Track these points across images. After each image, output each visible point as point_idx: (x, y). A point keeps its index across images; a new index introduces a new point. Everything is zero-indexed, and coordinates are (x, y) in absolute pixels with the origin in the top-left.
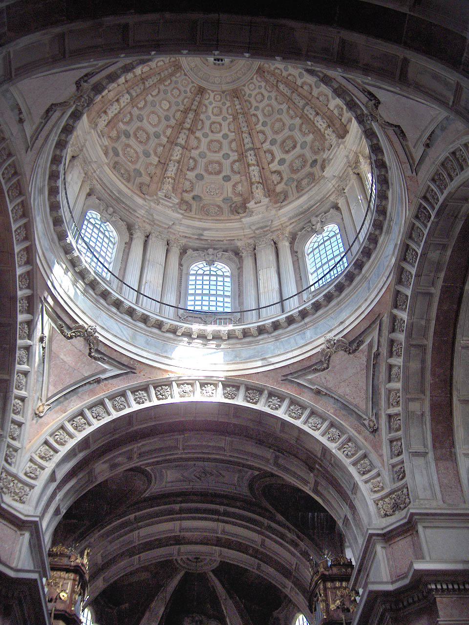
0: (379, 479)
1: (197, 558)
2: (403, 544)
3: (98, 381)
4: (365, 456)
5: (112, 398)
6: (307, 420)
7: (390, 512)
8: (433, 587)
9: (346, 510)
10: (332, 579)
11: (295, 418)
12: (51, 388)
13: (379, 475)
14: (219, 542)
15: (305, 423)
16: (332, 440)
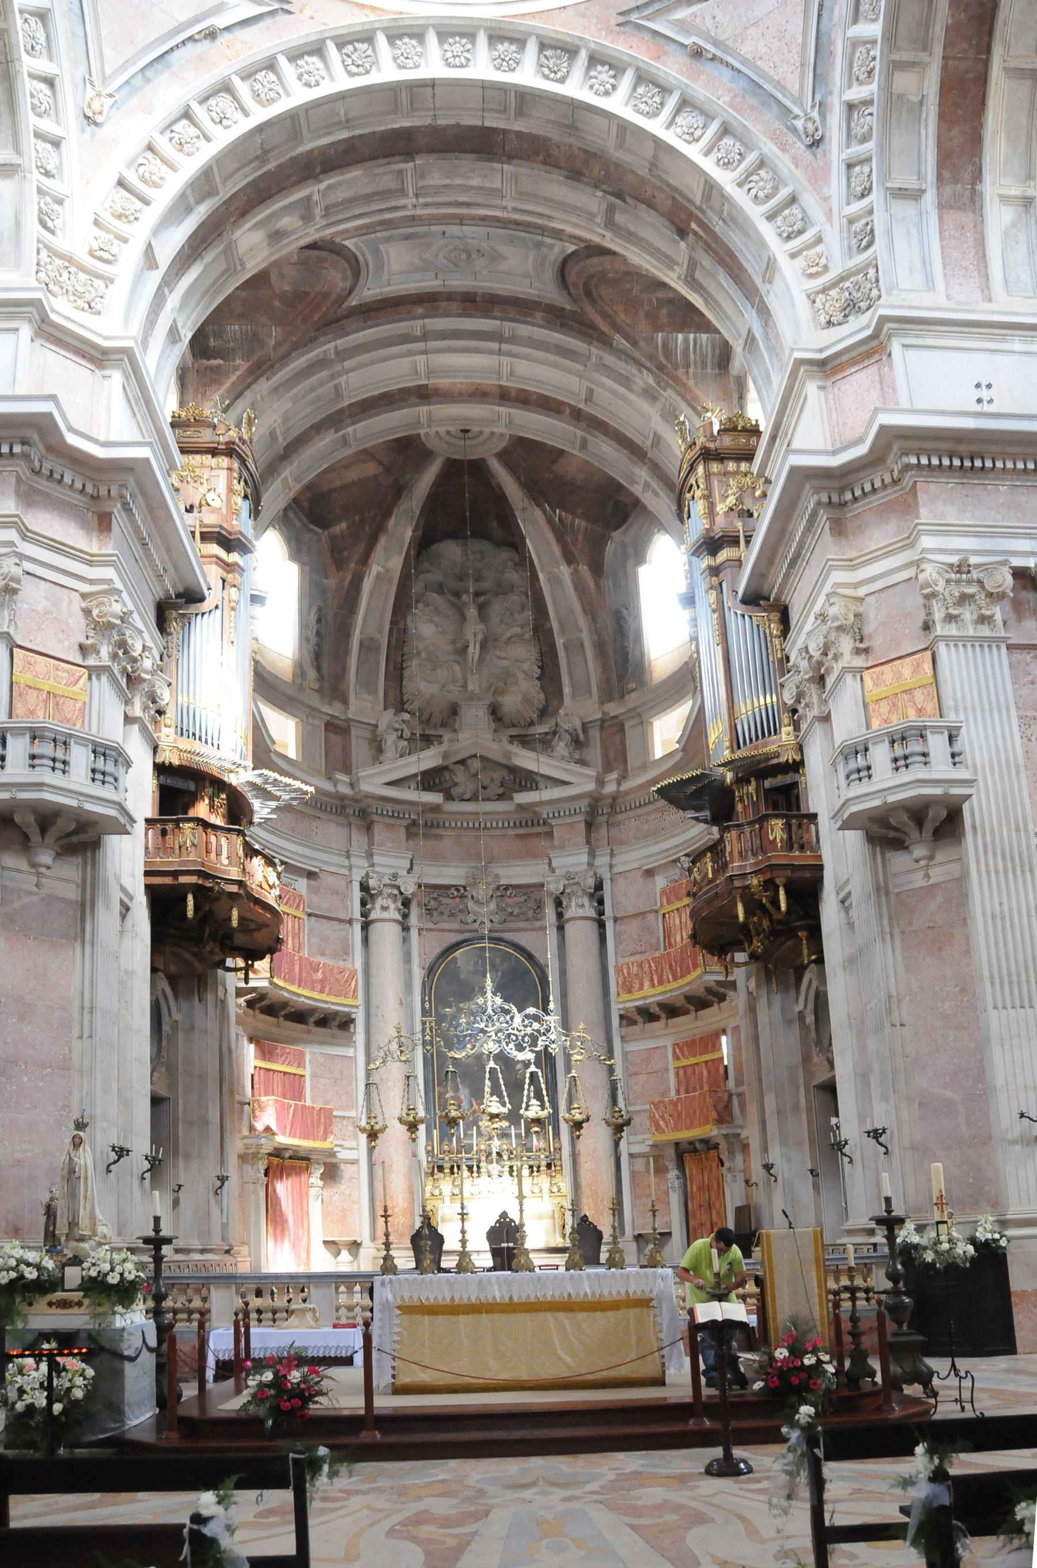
0: (819, 249)
1: (467, 431)
6: (674, 118)
7: (838, 317)
8: (914, 460)
9: (751, 318)
10: (719, 456)
11: (649, 115)
13: (819, 240)
14: (504, 396)
15: (670, 124)
16: (726, 164)
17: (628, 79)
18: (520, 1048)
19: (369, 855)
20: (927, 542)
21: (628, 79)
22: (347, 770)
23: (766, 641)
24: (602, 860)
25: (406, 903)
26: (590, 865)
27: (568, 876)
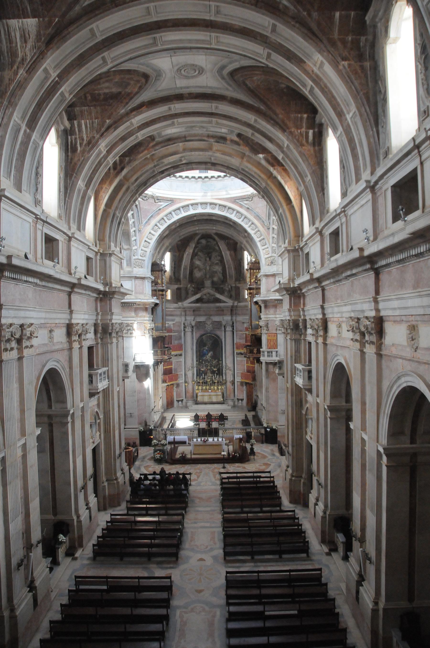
2: (271, 279)
3: (160, 209)
4: (264, 239)
5: (166, 216)
10: (253, 269)
12: (143, 219)
15: (243, 221)
17: (235, 212)
18: (214, 368)
20: (277, 316)
21: (235, 212)
23: (258, 311)
24: (234, 318)
26: (232, 319)
27: (227, 321)
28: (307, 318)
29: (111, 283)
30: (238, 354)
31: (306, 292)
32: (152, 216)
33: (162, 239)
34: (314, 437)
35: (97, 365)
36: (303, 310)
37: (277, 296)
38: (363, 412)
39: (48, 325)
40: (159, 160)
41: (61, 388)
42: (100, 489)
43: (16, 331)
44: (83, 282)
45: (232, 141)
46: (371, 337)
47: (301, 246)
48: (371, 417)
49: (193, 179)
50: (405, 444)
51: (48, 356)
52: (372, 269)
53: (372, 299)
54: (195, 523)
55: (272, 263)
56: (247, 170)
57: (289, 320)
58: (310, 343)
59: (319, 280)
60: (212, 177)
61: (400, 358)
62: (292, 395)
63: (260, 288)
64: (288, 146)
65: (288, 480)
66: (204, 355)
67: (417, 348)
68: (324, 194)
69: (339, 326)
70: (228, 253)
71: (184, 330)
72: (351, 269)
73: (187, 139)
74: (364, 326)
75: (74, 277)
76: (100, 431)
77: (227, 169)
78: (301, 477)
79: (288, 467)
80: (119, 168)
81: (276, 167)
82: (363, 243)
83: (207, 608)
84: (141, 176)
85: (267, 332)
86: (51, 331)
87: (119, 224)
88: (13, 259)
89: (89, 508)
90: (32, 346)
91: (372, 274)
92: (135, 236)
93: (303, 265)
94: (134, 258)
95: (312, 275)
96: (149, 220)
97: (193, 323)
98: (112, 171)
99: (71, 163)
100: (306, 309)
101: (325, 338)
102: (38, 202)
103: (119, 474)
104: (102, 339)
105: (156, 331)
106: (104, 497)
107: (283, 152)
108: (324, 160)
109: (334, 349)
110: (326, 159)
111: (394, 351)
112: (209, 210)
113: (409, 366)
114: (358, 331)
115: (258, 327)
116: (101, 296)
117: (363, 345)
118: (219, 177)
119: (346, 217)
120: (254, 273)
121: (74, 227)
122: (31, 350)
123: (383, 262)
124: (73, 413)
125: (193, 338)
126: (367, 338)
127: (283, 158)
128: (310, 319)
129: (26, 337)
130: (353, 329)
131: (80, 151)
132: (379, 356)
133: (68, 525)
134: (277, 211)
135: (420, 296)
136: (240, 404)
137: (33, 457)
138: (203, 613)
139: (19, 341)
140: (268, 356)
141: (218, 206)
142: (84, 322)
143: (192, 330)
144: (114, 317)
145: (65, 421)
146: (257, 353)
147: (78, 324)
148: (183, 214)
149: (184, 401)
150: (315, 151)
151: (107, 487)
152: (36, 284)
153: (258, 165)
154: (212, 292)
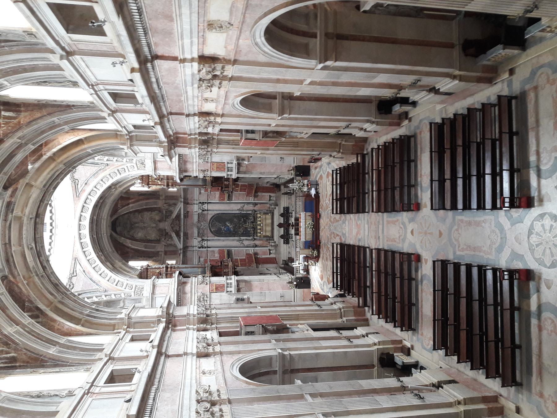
2: (159, 165)
3: (84, 271)
10: (149, 182)
17: (89, 197)
19: (194, 247)
20: (195, 161)
22: (177, 251)
24: (195, 202)
25: (203, 240)
28: (198, 131)
29: (158, 316)
30: (229, 199)
31: (172, 131)
32: (91, 279)
33: (114, 269)
34: (306, 130)
35: (237, 327)
36: (191, 135)
37: (176, 159)
38: (286, 82)
39: (198, 376)
40: (31, 271)
41: (257, 362)
42: (349, 325)
43: (203, 407)
44: (156, 343)
45: (12, 196)
46: (218, 69)
47: (127, 133)
48: (290, 75)
49: (53, 237)
50: (316, 44)
51: (228, 375)
52: (152, 62)
53: (182, 65)
54: (379, 238)
55: (142, 163)
56: (44, 183)
57: (199, 148)
58: (221, 130)
59: (161, 116)
60: (51, 218)
61: (238, 41)
62: (268, 150)
63: (168, 176)
64: (19, 138)
65: (343, 156)
66: (229, 229)
67: (229, 23)
68: (73, 106)
69: (206, 100)
70: (131, 205)
71: (205, 248)
72: (151, 83)
73: (7, 242)
74: (207, 74)
75: (151, 352)
76: (298, 324)
77: (43, 202)
78: (340, 144)
79: (331, 156)
80: (37, 313)
81: (43, 153)
82: (126, 69)
83: (456, 227)
84: (47, 289)
85: (209, 172)
86: (204, 373)
87: (97, 310)
88: (131, 414)
89: (367, 335)
90: (218, 391)
91: (157, 62)
92: (110, 295)
93: (146, 132)
94: (133, 295)
95: (156, 123)
96: (94, 282)
97: (200, 239)
98: (40, 320)
99: (28, 362)
100: (188, 132)
101: (216, 115)
102: (70, 394)
103: (335, 307)
104: (212, 324)
105: (205, 273)
106: (357, 320)
107: (26, 144)
108: (36, 102)
109: (227, 107)
110: (35, 100)
111: (231, 47)
112: (86, 223)
113: (246, 33)
114: (211, 81)
115: (204, 180)
116: (170, 326)
117: (225, 78)
118: (51, 212)
119: (98, 84)
120: (152, 181)
121: (99, 355)
122: (221, 392)
123: (146, 49)
124: (281, 349)
125: (213, 240)
126: (218, 73)
127: (33, 145)
128: (199, 128)
129: (210, 397)
130: (209, 86)
131: (15, 353)
132: (235, 62)
133: (382, 354)
134: (89, 155)
135: (180, 15)
136: (274, 198)
137: (322, 387)
138: (460, 231)
139: (213, 404)
140: (231, 171)
141: (82, 214)
142: (195, 341)
143: (205, 240)
144: (191, 312)
145: (288, 357)
146: (229, 181)
147: (197, 347)
148: (90, 248)
149: (270, 248)
150: (25, 111)
151: (347, 318)
152: (157, 389)
153: (39, 170)
154: (169, 221)
